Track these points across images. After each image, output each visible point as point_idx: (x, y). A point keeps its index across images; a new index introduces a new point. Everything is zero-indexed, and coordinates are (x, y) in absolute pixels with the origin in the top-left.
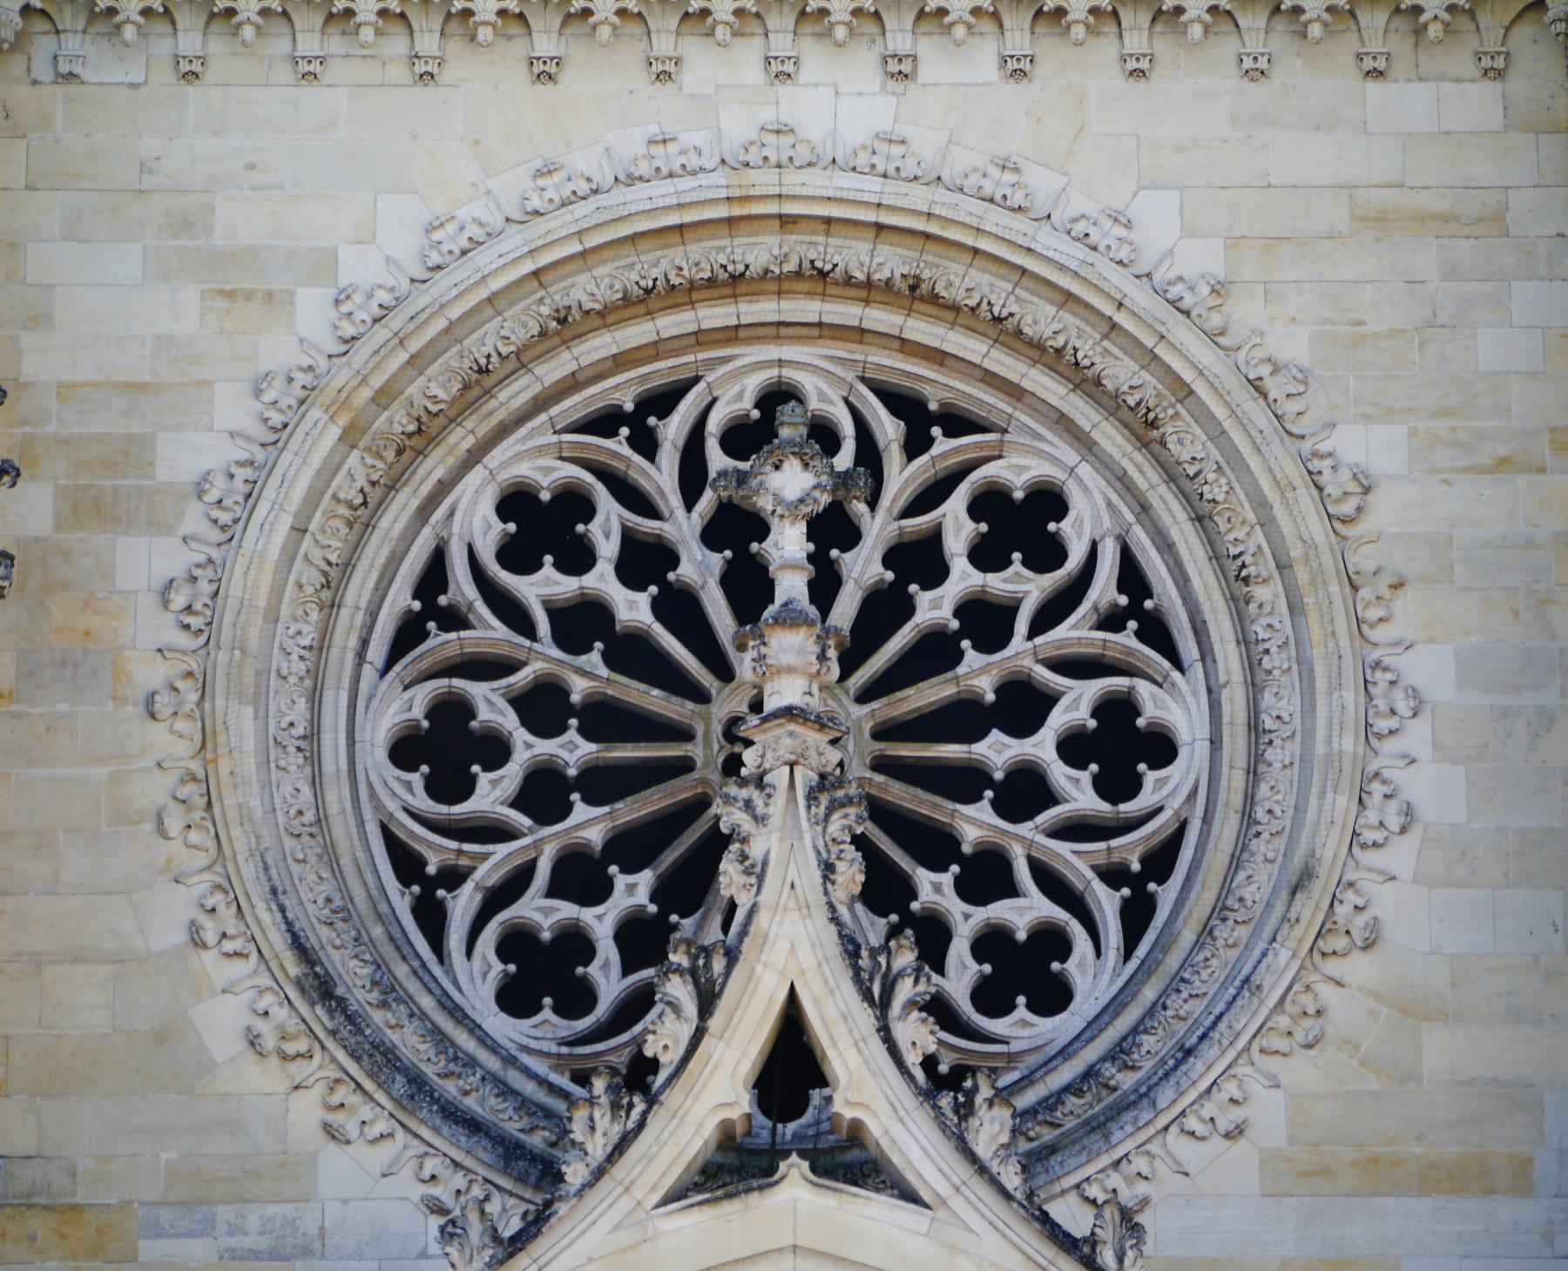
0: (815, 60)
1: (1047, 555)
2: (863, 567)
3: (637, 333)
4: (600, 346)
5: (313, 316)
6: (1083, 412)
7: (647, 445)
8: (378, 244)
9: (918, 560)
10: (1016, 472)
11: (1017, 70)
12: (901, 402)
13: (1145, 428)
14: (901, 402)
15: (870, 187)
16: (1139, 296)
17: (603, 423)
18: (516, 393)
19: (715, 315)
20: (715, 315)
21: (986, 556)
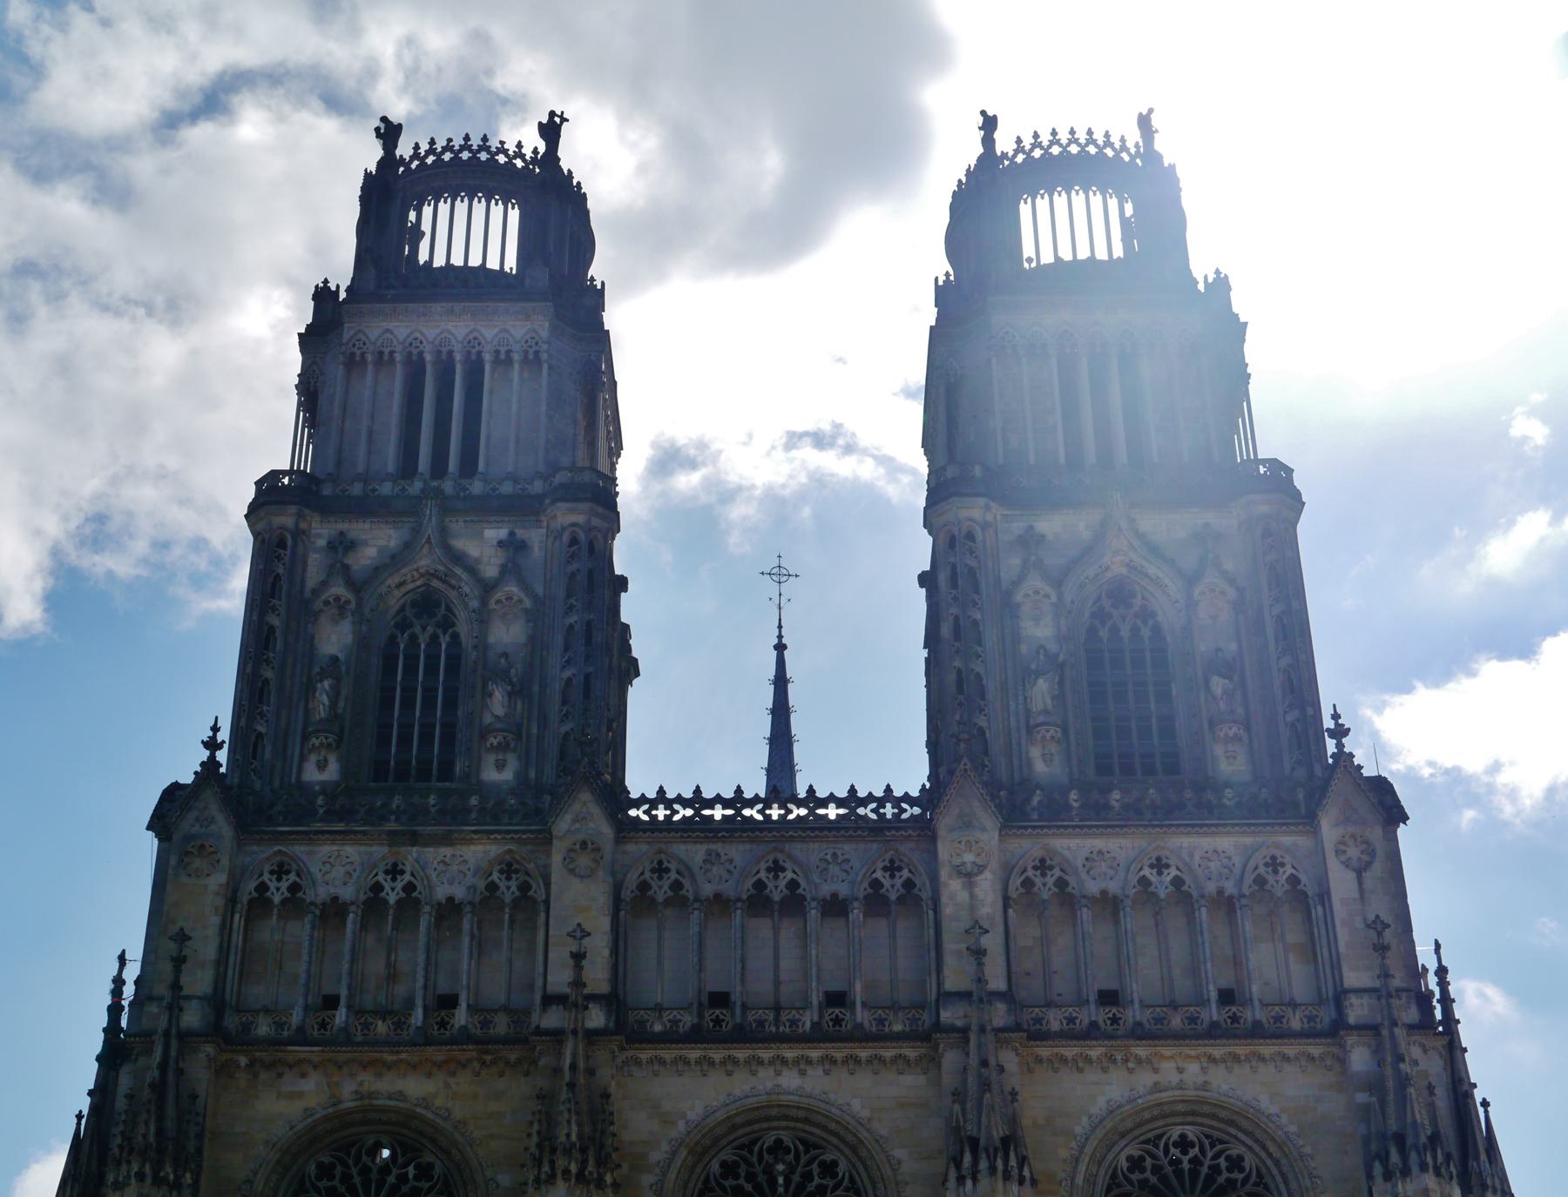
0: (785, 1072)
1: (834, 1175)
2: (796, 1178)
3: (749, 1129)
4: (741, 1132)
5: (681, 1125)
6: (842, 1146)
7: (751, 1152)
8: (695, 1112)
9: (808, 1177)
10: (828, 1157)
11: (827, 1073)
12: (803, 1142)
13: (854, 1150)
14: (803, 1142)
15: (795, 1098)
16: (853, 1122)
17: (741, 1147)
18: (724, 1142)
19: (765, 1125)
20: (765, 1125)
21: (822, 1175)
